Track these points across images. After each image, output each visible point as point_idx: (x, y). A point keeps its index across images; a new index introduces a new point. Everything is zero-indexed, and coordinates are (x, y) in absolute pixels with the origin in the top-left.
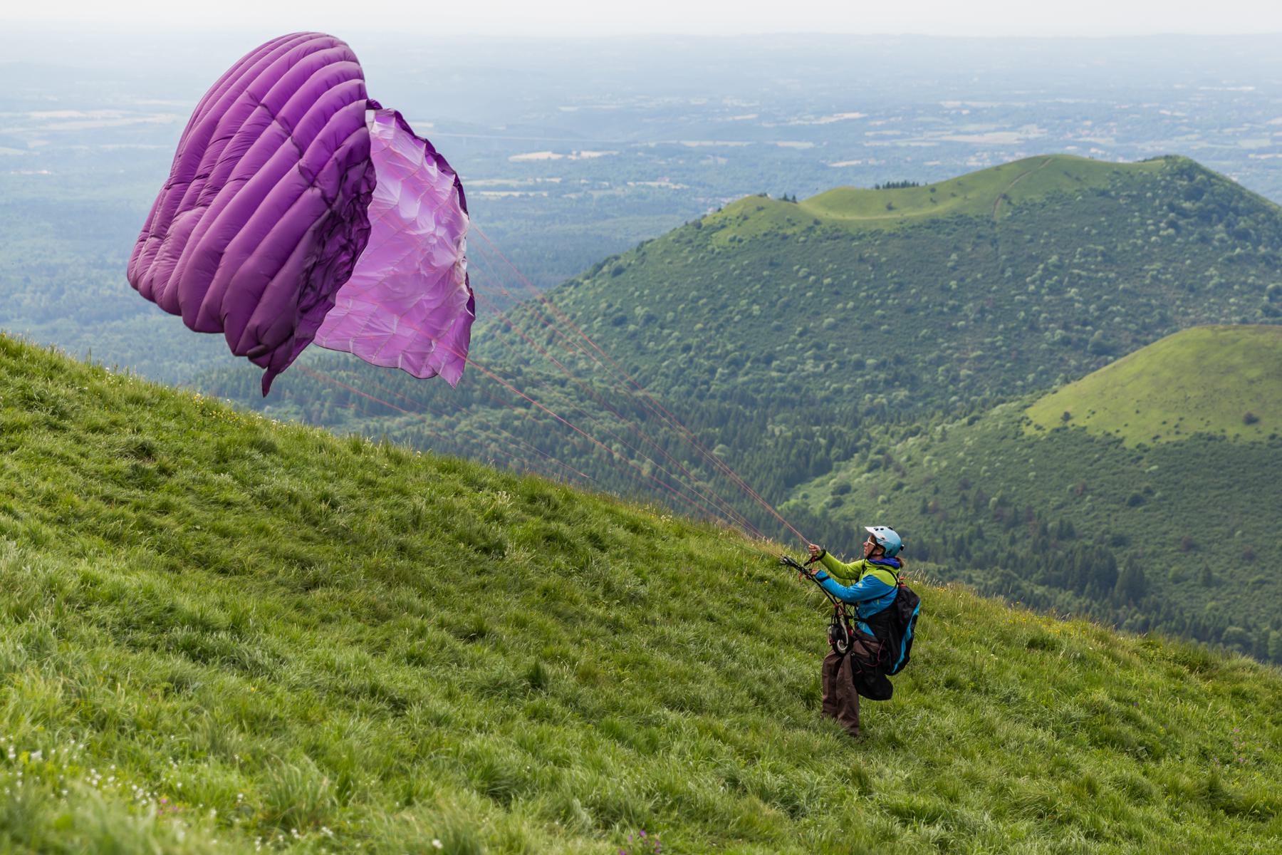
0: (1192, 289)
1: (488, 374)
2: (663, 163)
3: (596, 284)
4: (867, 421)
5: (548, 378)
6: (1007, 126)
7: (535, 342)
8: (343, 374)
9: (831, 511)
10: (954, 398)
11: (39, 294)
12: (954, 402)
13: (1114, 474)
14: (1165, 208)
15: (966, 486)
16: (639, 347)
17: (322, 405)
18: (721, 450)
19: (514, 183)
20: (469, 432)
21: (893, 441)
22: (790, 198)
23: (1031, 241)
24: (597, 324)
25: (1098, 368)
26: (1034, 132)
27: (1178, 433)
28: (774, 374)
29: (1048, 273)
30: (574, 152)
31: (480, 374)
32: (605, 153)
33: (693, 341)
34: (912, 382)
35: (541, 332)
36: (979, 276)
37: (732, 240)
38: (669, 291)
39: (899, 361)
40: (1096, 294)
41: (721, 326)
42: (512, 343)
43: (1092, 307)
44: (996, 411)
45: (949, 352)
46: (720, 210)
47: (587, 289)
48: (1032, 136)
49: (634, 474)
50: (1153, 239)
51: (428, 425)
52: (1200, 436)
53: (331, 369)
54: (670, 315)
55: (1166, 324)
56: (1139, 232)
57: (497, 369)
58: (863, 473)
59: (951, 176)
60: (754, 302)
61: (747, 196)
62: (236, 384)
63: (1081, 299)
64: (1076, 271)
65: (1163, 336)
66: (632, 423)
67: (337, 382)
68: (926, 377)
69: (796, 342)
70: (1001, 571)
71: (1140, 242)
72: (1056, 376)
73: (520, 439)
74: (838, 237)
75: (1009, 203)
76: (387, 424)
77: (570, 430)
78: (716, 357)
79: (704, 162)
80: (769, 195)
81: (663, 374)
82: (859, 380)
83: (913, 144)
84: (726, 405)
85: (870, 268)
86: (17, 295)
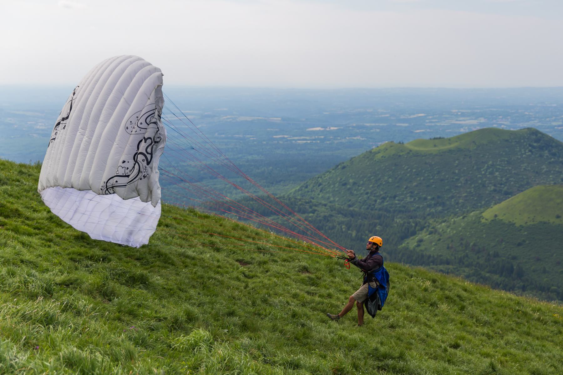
0: (537, 173)
1: (300, 203)
2: (358, 131)
4: (428, 217)
5: (320, 204)
6: (474, 118)
8: (251, 203)
9: (416, 248)
10: (457, 210)
12: (458, 211)
13: (512, 235)
14: (528, 145)
15: (462, 239)
16: (351, 193)
18: (379, 228)
19: (308, 138)
20: (294, 222)
21: (437, 224)
22: (401, 143)
23: (483, 157)
24: (337, 185)
25: (506, 199)
26: (482, 120)
27: (533, 221)
28: (397, 202)
29: (488, 168)
30: (328, 128)
31: (298, 202)
33: (369, 191)
34: (443, 204)
35: (318, 188)
36: (465, 168)
37: (382, 157)
39: (439, 197)
40: (505, 174)
41: (379, 186)
42: (308, 192)
43: (504, 179)
44: (472, 214)
45: (455, 194)
46: (378, 147)
48: (482, 121)
50: (524, 156)
51: (280, 219)
52: (541, 222)
53: (247, 201)
54: (361, 182)
55: (529, 184)
56: (519, 153)
57: (303, 201)
58: (427, 235)
59: (455, 135)
60: (390, 178)
61: (387, 142)
62: (215, 206)
63: (499, 176)
64: (498, 167)
65: (527, 189)
66: (349, 219)
68: (448, 203)
69: (404, 191)
70: (474, 268)
71: (519, 157)
72: (492, 202)
74: (417, 156)
75: (475, 144)
76: (266, 220)
77: (328, 221)
78: (377, 196)
79: (372, 131)
80: (395, 142)
82: (425, 204)
83: (442, 124)
84: (381, 212)
85: (428, 166)
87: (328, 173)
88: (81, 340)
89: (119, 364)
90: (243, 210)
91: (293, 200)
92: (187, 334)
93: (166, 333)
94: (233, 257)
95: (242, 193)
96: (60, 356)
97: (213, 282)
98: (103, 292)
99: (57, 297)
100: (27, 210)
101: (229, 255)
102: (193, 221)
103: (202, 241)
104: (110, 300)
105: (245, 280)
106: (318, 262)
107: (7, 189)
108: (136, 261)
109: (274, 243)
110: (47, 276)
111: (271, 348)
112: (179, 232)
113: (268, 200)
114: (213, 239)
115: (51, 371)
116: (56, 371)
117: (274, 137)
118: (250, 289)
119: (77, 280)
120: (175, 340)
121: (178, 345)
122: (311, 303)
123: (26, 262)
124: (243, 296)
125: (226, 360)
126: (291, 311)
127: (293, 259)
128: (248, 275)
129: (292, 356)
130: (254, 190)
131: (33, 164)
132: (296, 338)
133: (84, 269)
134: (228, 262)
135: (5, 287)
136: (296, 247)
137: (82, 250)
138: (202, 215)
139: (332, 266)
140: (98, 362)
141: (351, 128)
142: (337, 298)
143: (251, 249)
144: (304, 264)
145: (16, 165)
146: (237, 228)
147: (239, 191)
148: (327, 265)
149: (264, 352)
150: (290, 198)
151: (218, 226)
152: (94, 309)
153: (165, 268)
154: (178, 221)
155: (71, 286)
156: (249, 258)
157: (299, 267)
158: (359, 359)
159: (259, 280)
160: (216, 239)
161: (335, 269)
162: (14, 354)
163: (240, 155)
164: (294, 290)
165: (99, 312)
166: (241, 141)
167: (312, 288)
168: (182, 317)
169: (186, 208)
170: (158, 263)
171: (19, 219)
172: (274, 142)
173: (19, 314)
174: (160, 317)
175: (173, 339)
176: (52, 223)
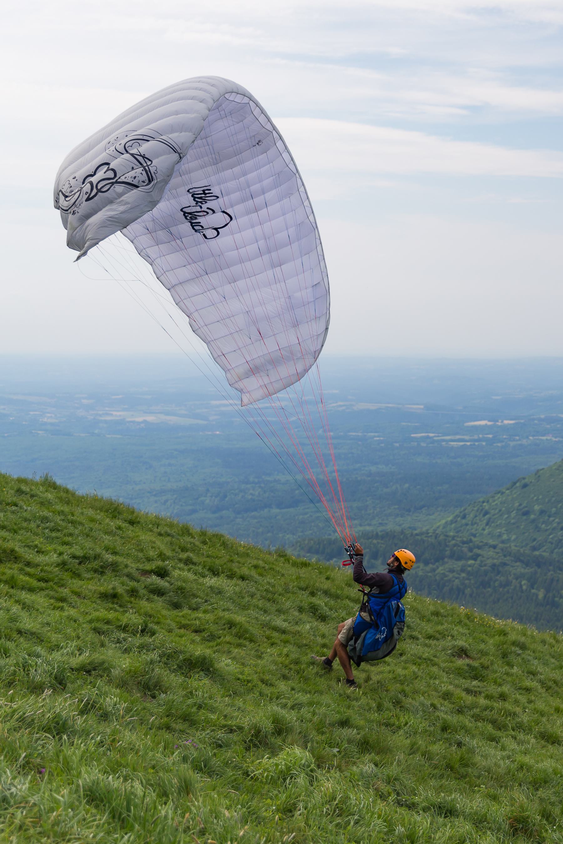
1: (453, 542)
2: (548, 426)
3: (513, 492)
5: (486, 544)
7: (480, 524)
8: (375, 541)
11: (214, 498)
19: (467, 438)
20: (443, 574)
24: (513, 514)
30: (500, 421)
31: (449, 542)
32: (517, 421)
35: (482, 519)
38: (553, 497)
47: (508, 495)
49: (534, 598)
53: (368, 538)
54: (554, 510)
57: (459, 539)
62: (318, 546)
66: (533, 569)
67: (372, 546)
73: (471, 577)
81: (550, 542)
86: (202, 498)
87: (499, 495)
89: (168, 801)
91: (442, 537)
92: (274, 753)
95: (361, 525)
96: (78, 786)
97: (315, 670)
98: (143, 683)
100: (29, 551)
102: (283, 572)
104: (154, 697)
106: (483, 641)
108: (194, 634)
110: (57, 656)
112: (261, 588)
113: (402, 537)
114: (315, 600)
115: (65, 809)
116: (72, 810)
117: (412, 435)
119: (103, 663)
120: (255, 763)
121: (260, 771)
122: (473, 708)
123: (25, 633)
124: (363, 694)
125: (337, 800)
126: (439, 720)
127: (443, 635)
129: (443, 795)
130: (380, 521)
131: (38, 479)
132: (450, 767)
133: (114, 646)
136: (448, 615)
137: (111, 615)
138: (298, 561)
139: (508, 648)
140: (136, 796)
141: (536, 422)
142: (515, 701)
144: (461, 643)
145: (13, 480)
148: (499, 646)
149: (398, 787)
150: (437, 534)
151: (323, 580)
152: (128, 710)
153: (239, 645)
154: (259, 570)
155: (93, 672)
158: (553, 804)
159: (388, 668)
160: (320, 601)
161: (511, 653)
162: (9, 782)
164: (445, 686)
166: (360, 443)
167: (475, 683)
168: (267, 726)
169: (273, 549)
170: (228, 638)
171: (16, 565)
172: (412, 443)
173: (16, 717)
174: (232, 726)
175: (253, 762)
176: (66, 571)
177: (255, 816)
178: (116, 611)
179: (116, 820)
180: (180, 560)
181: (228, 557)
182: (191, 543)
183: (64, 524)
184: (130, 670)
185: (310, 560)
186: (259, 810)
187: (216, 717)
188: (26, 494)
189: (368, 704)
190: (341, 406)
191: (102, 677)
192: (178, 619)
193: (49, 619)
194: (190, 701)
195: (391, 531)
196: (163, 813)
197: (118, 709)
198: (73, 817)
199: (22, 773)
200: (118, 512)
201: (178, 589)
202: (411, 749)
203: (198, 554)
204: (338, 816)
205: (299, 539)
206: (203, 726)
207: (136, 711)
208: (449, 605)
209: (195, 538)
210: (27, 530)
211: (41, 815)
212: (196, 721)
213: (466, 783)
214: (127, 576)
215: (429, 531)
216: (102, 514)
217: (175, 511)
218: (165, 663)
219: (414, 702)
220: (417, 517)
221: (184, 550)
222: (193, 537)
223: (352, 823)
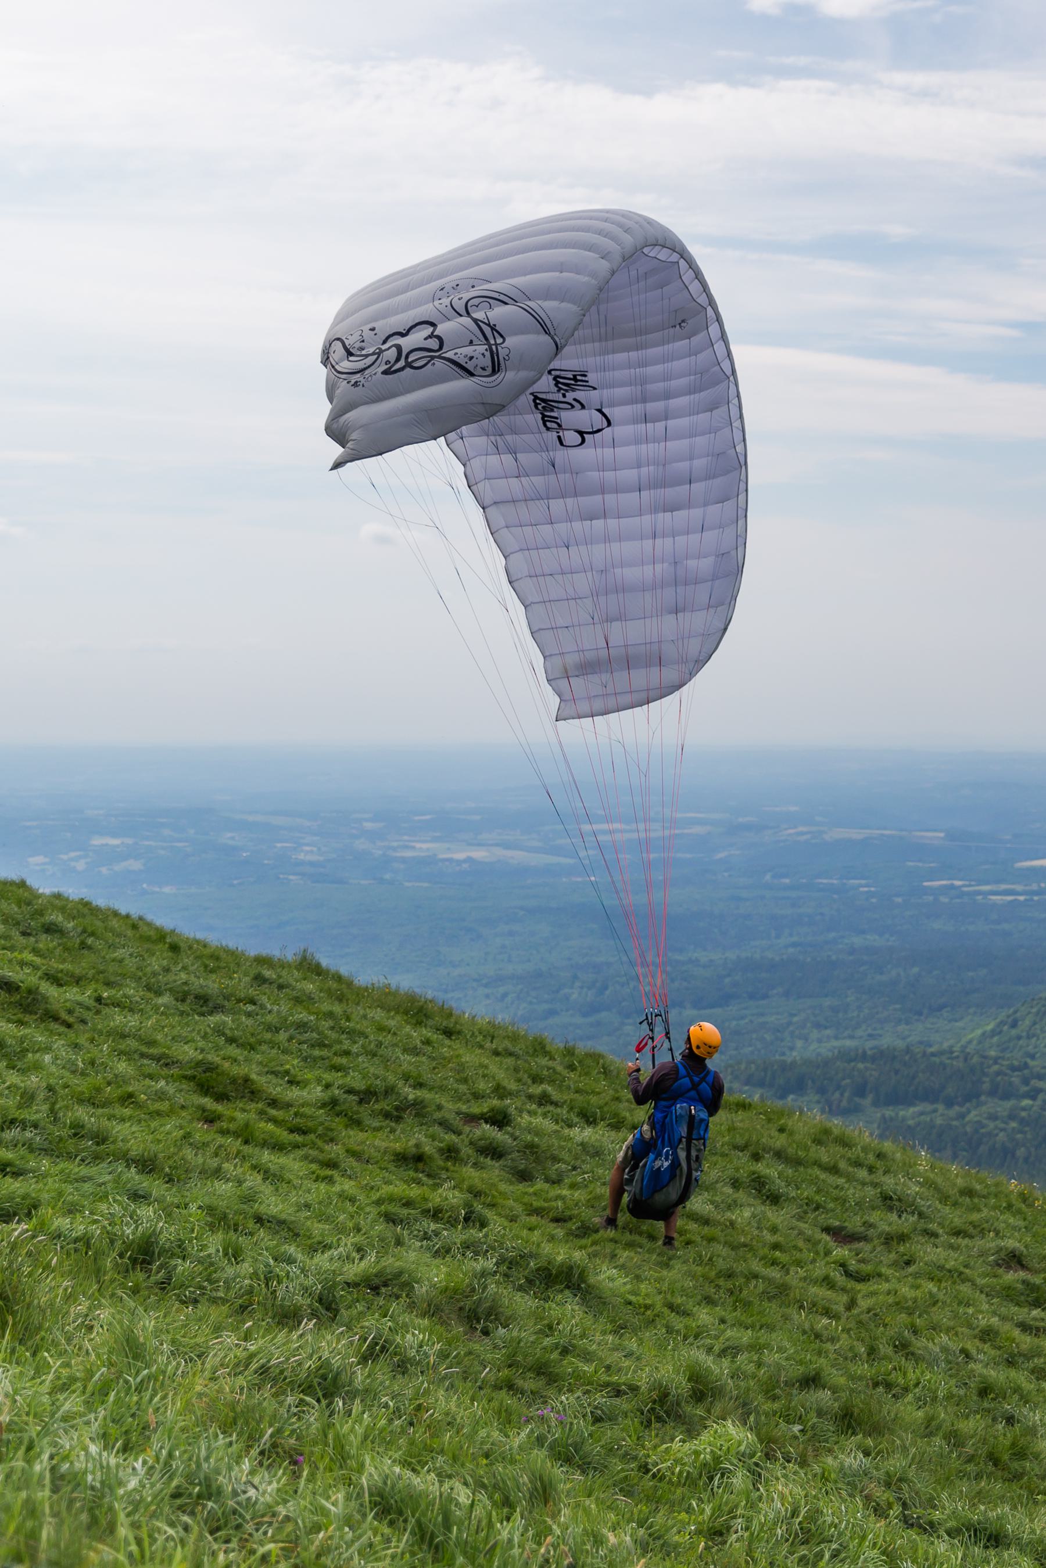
1: (996, 1068)
7: (1041, 1037)
8: (861, 1066)
11: (585, 990)
17: (842, 1095)
19: (1019, 888)
20: (978, 1122)
31: (989, 1067)
42: (1019, 1038)
51: (940, 1115)
53: (850, 1061)
57: (1006, 1063)
67: (856, 1073)
73: (1027, 1129)
76: (901, 1113)
86: (566, 991)
88: (412, 1443)
89: (512, 1514)
90: (838, 1087)
91: (975, 1059)
92: (691, 1433)
93: (635, 1431)
94: (816, 1218)
95: (836, 1038)
96: (362, 1488)
97: (761, 1287)
99: (347, 1320)
101: (802, 1214)
103: (730, 1172)
104: (486, 1333)
105: (849, 1286)
107: (224, 1023)
108: (555, 1225)
109: (928, 1184)
110: (322, 1260)
111: (923, 1484)
113: (907, 1058)
114: (760, 1167)
115: (340, 1529)
117: (925, 884)
118: (862, 1313)
119: (400, 1274)
120: (659, 1449)
121: (669, 1464)
122: (1033, 1356)
123: (269, 1221)
124: (843, 1330)
128: (857, 1272)
129: (982, 1508)
130: (870, 1031)
131: (290, 956)
134: (801, 1233)
135: (217, 1290)
136: (989, 1194)
137: (414, 1192)
143: (865, 1197)
144: (1011, 1243)
145: (246, 960)
146: (825, 1138)
147: (828, 1032)
152: (443, 1355)
155: (383, 1290)
156: (859, 1224)
157: (997, 1252)
159: (886, 1286)
160: (769, 1169)
162: (244, 1479)
163: (832, 935)
164: (983, 1318)
165: (458, 1363)
166: (835, 896)
167: (1035, 1313)
168: (680, 1385)
171: (253, 1105)
173: (254, 1366)
174: (619, 1385)
175: (655, 1447)
176: (338, 1115)
177: (662, 1542)
178: (419, 1182)
179: (425, 1547)
180: (530, 1097)
181: (611, 1092)
182: (549, 1069)
183: (334, 1035)
184: (446, 1289)
185: (750, 1096)
186: (667, 1531)
187: (593, 1368)
188: (271, 983)
189: (851, 1348)
190: (802, 833)
191: (398, 1297)
192: (526, 1199)
193: (309, 1198)
194: (547, 1341)
195: (888, 1048)
196: (505, 1535)
197: (425, 1353)
198: (353, 1542)
199: (266, 1463)
200: (425, 1015)
201: (526, 1147)
202: (926, 1428)
203: (560, 1086)
204: (803, 1544)
205: (730, 1062)
206: (570, 1384)
207: (455, 1357)
208: (987, 1179)
209: (555, 1060)
210: (272, 1044)
211: (297, 1538)
212: (557, 1375)
213: (1021, 1488)
214: (440, 1124)
215: (955, 1049)
216: (398, 1018)
217: (520, 1013)
218: (506, 1275)
219: (930, 1345)
220: (932, 1024)
221: (536, 1079)
222: (552, 1058)
223: (827, 1556)
